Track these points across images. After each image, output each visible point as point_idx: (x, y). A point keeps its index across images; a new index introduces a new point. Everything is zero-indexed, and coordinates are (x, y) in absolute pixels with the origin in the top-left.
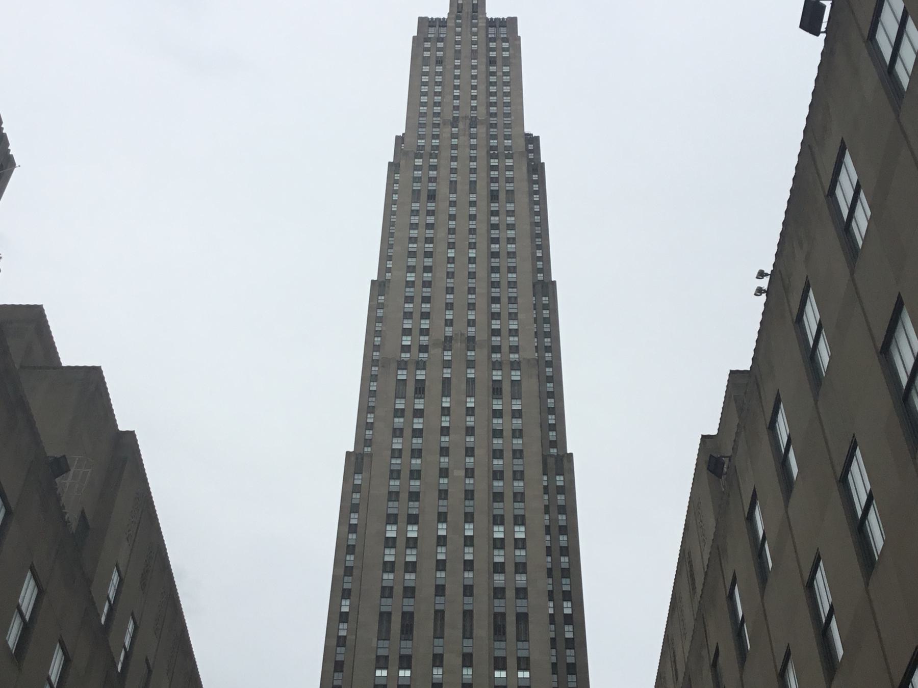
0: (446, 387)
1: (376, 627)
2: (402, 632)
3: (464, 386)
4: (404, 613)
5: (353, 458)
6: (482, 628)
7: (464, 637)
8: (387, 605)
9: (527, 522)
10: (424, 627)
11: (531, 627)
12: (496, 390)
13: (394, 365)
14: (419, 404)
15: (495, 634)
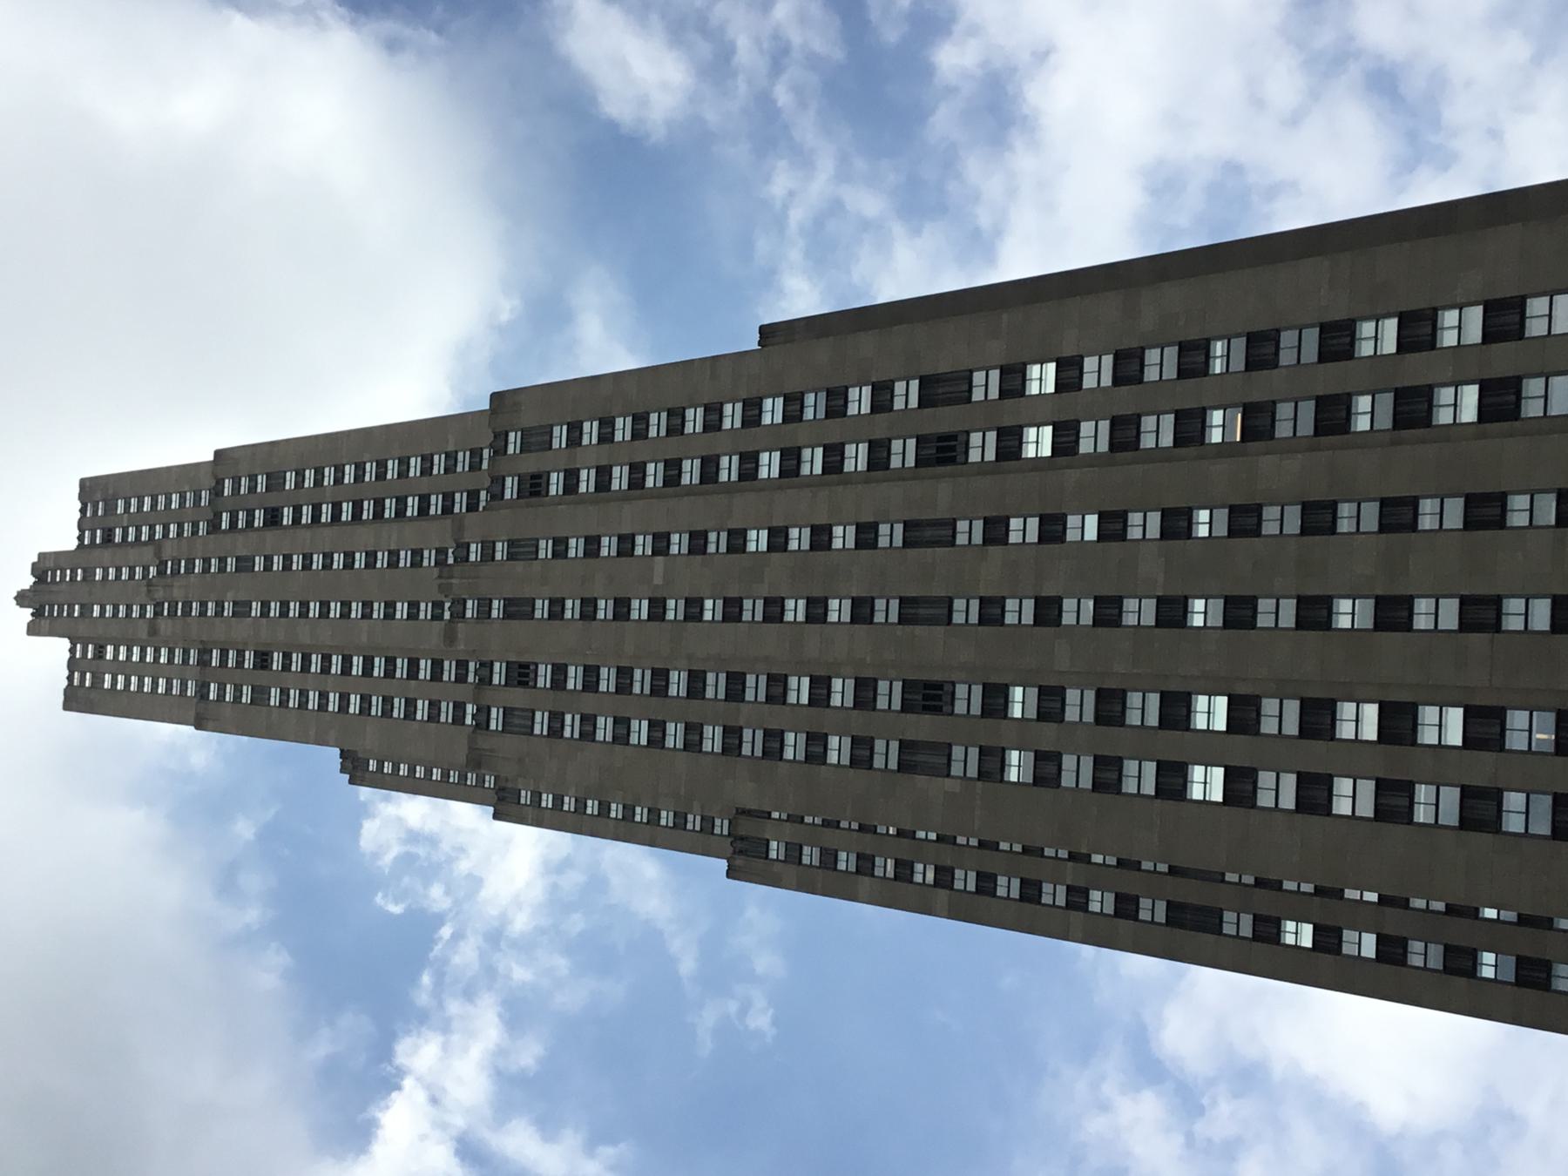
0: (518, 609)
1: (921, 780)
2: (937, 710)
3: (519, 566)
4: (906, 707)
5: (739, 861)
6: (940, 495)
7: (952, 542)
8: (886, 754)
9: (754, 394)
10: (932, 650)
11: (943, 368)
12: (534, 486)
13: (484, 742)
14: (544, 677)
15: (952, 461)
